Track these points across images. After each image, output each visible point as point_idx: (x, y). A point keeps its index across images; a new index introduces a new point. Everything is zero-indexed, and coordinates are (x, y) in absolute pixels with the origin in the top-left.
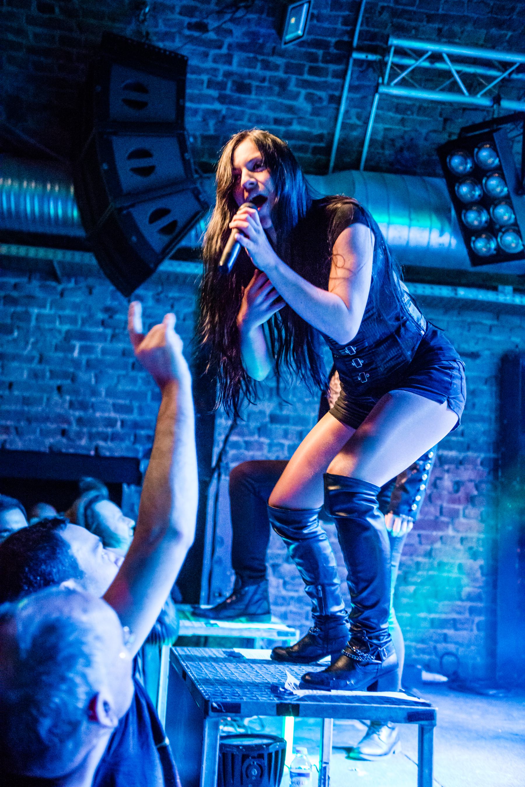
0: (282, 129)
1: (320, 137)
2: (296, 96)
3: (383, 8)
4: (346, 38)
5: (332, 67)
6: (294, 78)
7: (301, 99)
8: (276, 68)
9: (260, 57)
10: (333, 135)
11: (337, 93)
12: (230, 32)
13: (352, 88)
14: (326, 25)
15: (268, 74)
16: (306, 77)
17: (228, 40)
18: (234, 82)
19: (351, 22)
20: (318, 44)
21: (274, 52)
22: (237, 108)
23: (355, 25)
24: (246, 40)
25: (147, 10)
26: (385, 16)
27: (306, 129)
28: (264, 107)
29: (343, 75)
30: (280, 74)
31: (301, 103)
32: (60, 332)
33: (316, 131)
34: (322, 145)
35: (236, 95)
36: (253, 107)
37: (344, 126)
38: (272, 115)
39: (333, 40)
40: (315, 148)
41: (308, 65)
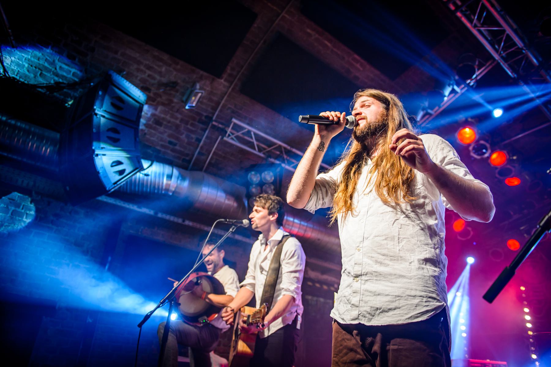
0: (171, 146)
1: (187, 155)
2: (182, 134)
3: (230, 108)
4: (210, 115)
5: (201, 126)
6: (183, 125)
7: (184, 136)
8: (177, 118)
9: (171, 112)
10: (193, 155)
11: (200, 138)
12: (161, 96)
13: (207, 137)
14: (204, 107)
15: (172, 120)
16: (189, 126)
17: (159, 99)
18: (155, 119)
19: (215, 109)
20: (198, 114)
21: (178, 111)
22: (153, 131)
23: (216, 111)
24: (166, 102)
25: (125, 73)
26: (229, 111)
27: (182, 150)
28: (166, 135)
29: (204, 130)
30: (178, 122)
31: (183, 137)
32: (25, 222)
33: (186, 152)
34: (188, 158)
35: (154, 125)
36: (161, 133)
37: (199, 153)
38: (168, 139)
39: (205, 114)
40: (184, 159)
41: (191, 122)
